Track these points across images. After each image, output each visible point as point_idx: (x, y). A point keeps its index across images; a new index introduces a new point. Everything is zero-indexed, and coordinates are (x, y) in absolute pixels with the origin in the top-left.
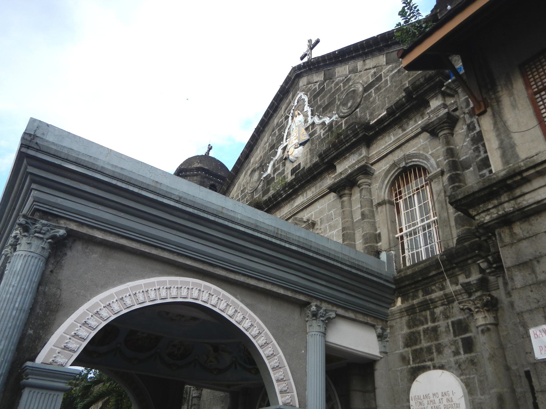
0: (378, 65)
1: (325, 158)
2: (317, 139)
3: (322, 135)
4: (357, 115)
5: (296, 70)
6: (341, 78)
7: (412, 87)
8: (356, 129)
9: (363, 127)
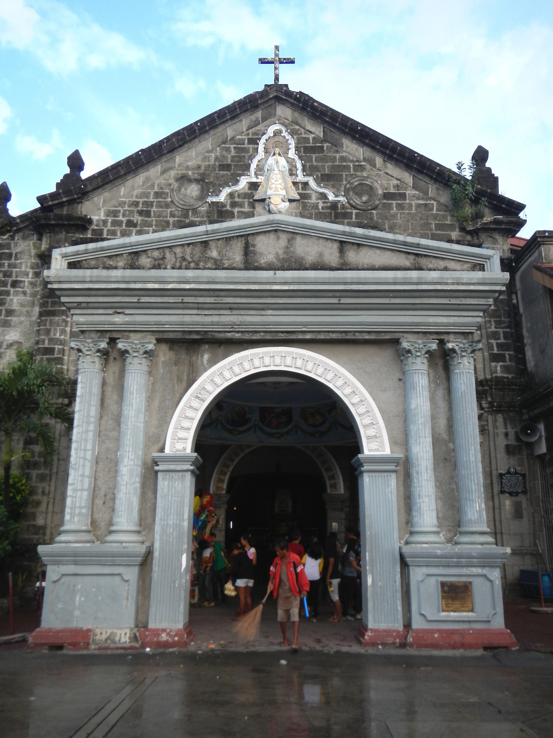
0: (402, 180)
2: (313, 207)
3: (320, 207)
4: (373, 217)
6: (351, 158)
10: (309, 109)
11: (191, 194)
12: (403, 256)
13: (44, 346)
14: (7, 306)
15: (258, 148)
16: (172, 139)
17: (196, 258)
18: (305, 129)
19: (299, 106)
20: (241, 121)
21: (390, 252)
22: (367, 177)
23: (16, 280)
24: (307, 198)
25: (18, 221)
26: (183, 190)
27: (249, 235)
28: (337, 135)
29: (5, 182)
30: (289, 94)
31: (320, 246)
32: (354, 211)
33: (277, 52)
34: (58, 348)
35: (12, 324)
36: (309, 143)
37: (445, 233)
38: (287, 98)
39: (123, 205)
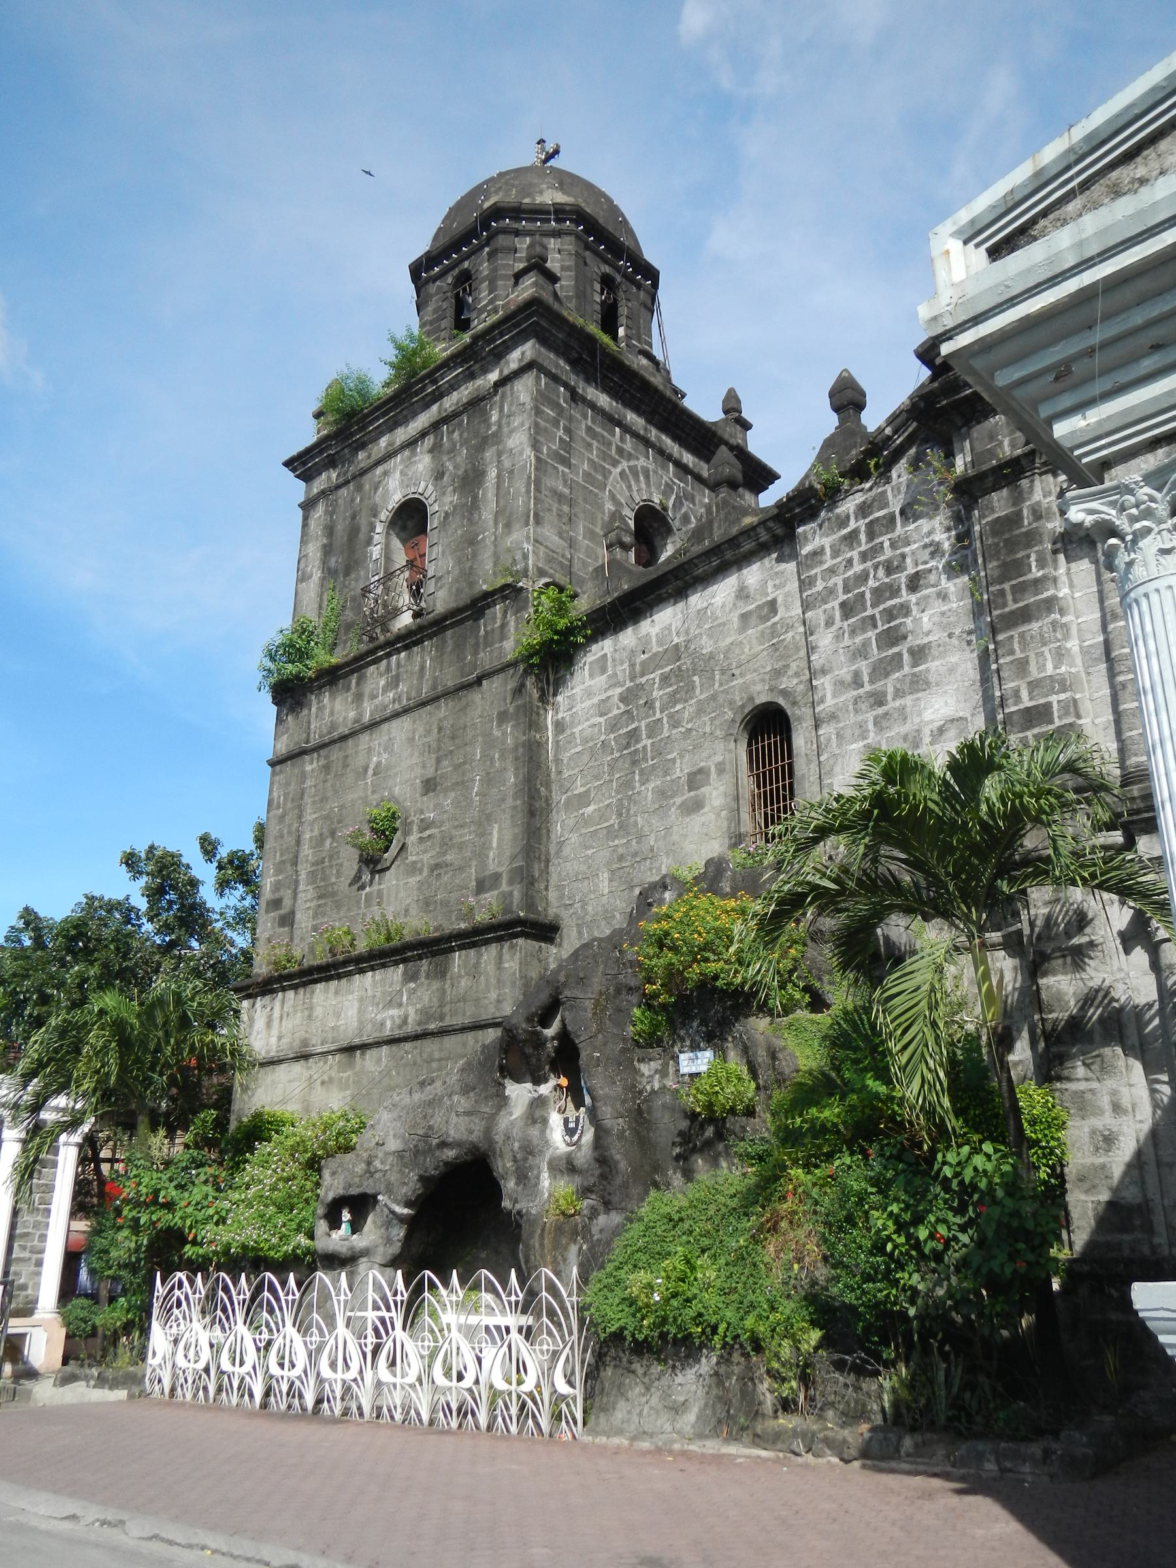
13: (1021, 706)
14: (911, 641)
23: (917, 572)
25: (888, 431)
29: (846, 370)
34: (1059, 702)
35: (932, 678)
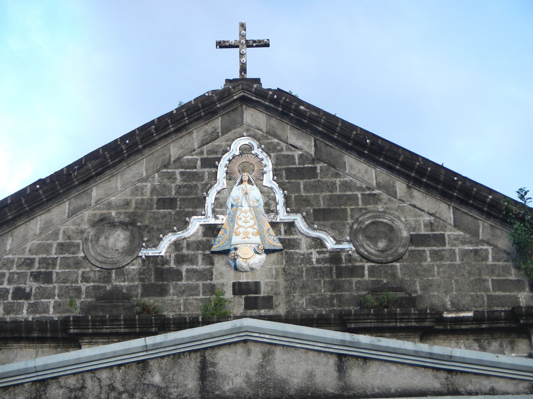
0: (438, 215)
1: (352, 321)
2: (302, 260)
3: (314, 260)
4: (396, 273)
5: (251, 92)
6: (358, 184)
7: (526, 311)
8: (426, 314)
9: (438, 316)
10: (292, 115)
11: (115, 245)
12: (430, 373)
15: (216, 173)
16: (86, 164)
17: (130, 386)
18: (287, 143)
19: (278, 110)
20: (191, 133)
21: (410, 369)
22: (384, 212)
24: (293, 247)
26: (102, 239)
27: (206, 349)
28: (335, 151)
30: (263, 94)
31: (310, 362)
32: (367, 265)
33: (243, 32)
36: (294, 163)
37: (508, 294)
38: (259, 100)
39: (9, 265)
